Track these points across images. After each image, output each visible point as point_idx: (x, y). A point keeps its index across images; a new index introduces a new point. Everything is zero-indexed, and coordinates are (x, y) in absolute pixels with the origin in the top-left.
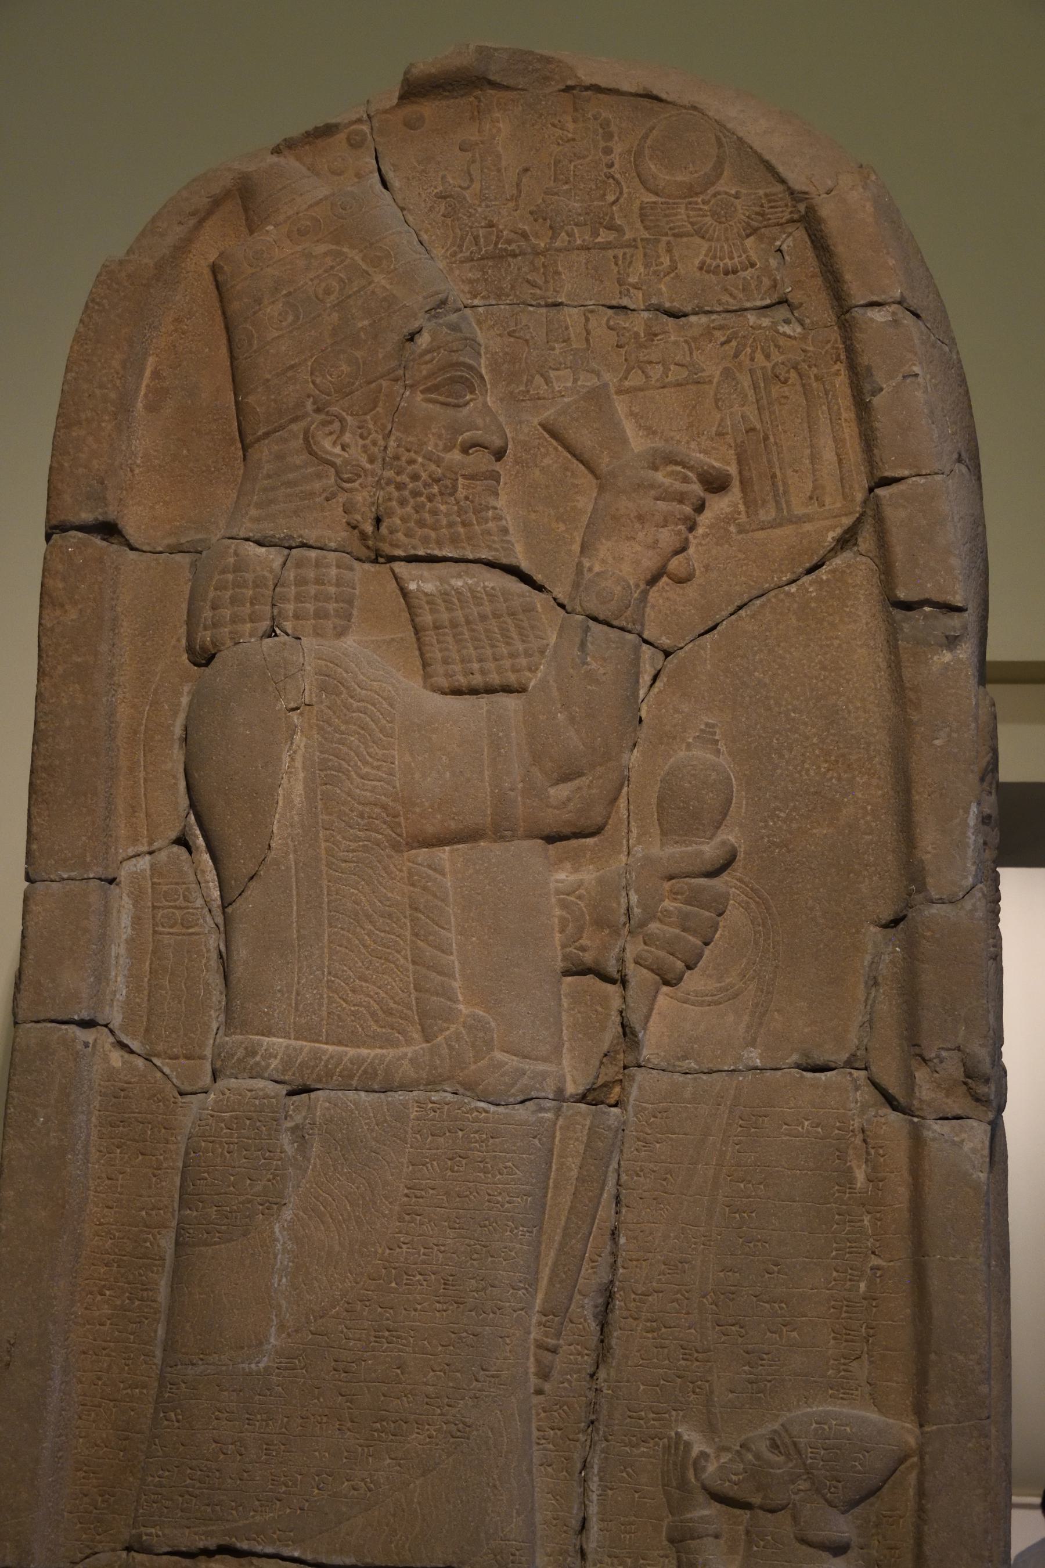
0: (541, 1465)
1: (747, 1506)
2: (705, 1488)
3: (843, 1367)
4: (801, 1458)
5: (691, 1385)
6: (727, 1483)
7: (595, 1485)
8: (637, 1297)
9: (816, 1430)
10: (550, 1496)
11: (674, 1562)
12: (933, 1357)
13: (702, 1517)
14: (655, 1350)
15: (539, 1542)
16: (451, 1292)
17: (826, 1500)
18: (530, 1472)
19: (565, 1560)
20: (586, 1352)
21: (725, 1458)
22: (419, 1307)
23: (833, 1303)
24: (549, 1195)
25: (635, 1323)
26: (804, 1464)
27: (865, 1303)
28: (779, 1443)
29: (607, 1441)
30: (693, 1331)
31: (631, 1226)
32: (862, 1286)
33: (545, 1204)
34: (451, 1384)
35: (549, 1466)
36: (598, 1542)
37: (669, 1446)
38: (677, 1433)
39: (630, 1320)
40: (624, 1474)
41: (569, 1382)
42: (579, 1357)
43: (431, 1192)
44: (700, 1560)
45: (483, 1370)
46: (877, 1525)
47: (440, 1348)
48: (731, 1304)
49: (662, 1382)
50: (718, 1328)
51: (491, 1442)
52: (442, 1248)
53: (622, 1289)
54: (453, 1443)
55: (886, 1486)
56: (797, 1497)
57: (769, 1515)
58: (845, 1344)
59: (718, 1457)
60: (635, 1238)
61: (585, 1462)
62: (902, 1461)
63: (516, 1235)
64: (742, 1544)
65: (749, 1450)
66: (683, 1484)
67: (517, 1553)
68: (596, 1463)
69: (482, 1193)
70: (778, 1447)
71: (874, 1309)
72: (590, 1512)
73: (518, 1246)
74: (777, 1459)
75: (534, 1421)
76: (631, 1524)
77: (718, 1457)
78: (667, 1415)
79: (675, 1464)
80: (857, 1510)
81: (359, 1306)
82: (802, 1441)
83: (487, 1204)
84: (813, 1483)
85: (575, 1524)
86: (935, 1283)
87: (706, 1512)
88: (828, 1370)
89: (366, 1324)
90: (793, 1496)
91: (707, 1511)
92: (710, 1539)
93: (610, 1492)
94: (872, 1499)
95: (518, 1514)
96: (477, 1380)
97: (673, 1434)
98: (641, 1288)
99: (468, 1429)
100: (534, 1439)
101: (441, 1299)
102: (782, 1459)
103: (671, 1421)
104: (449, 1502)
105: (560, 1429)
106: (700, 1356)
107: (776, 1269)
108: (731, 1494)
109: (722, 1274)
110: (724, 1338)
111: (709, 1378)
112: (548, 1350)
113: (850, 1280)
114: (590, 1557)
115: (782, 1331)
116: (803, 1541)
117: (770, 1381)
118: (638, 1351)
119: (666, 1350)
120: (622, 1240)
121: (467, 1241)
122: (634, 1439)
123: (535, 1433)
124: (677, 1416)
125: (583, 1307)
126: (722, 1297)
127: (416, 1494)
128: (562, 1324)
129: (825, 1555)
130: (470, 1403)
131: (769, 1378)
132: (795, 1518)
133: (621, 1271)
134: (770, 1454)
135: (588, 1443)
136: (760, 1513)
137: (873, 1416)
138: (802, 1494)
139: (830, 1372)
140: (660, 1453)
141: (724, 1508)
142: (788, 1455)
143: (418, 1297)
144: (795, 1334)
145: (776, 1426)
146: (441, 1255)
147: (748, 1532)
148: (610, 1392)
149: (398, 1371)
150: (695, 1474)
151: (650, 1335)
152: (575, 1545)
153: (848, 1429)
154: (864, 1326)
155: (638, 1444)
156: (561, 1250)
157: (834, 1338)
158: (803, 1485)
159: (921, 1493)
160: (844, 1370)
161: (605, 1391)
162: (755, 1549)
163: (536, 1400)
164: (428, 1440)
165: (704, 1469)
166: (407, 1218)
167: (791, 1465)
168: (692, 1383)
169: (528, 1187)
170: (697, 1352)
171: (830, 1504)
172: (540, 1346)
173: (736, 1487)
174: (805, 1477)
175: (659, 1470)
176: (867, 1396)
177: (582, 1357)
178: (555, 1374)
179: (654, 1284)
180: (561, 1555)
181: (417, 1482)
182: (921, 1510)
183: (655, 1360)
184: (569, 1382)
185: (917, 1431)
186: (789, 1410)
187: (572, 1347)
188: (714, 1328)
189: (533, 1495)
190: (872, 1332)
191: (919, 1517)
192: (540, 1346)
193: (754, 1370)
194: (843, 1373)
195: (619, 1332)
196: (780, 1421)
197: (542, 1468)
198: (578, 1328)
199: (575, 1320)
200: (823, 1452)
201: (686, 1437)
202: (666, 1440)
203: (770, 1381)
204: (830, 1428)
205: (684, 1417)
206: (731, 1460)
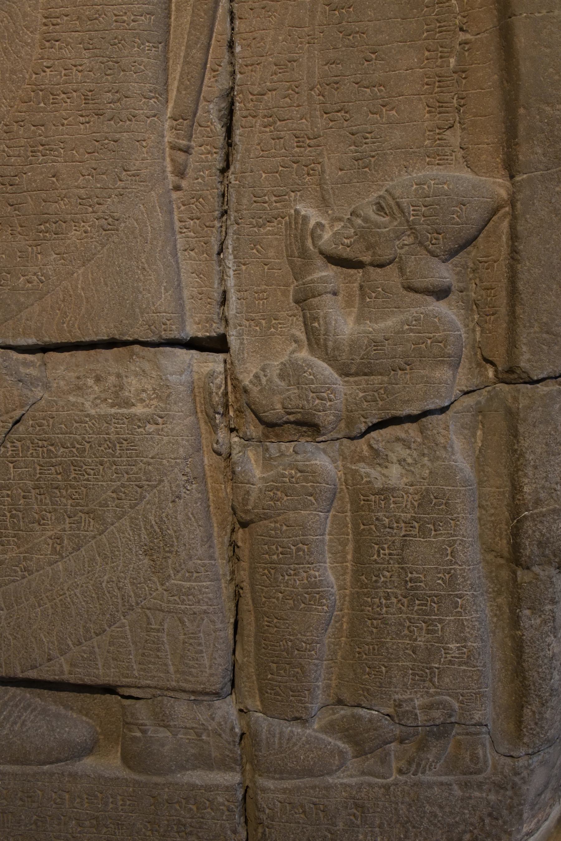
0: (185, 250)
1: (358, 265)
2: (321, 253)
3: (437, 137)
4: (404, 216)
5: (305, 168)
6: (341, 247)
7: (231, 262)
8: (254, 97)
9: (416, 190)
10: (194, 275)
11: (301, 319)
12: (522, 111)
13: (321, 278)
14: (273, 142)
15: (188, 314)
16: (91, 106)
17: (429, 251)
18: (175, 255)
19: (212, 325)
20: (215, 150)
21: (338, 226)
22: (66, 122)
23: (426, 80)
24: (173, 18)
25: (254, 120)
26: (408, 221)
27: (455, 76)
28: (384, 204)
29: (238, 224)
30: (304, 121)
31: (244, 35)
32: (452, 61)
33: (170, 25)
34: (99, 186)
35: (192, 250)
36: (237, 308)
37: (290, 223)
38: (296, 210)
39: (250, 118)
40: (255, 251)
41: (203, 177)
42: (209, 156)
43: (65, 18)
44: (322, 314)
45: (126, 171)
46: (474, 271)
47: (87, 155)
48: (336, 93)
49: (281, 168)
50: (325, 116)
51: (137, 231)
52: (80, 68)
53: (241, 92)
54: (105, 235)
55: (482, 235)
56: (403, 251)
57: (379, 270)
58: (438, 116)
59: (332, 226)
60: (249, 45)
61: (222, 244)
62: (495, 212)
63: (143, 50)
64: (357, 298)
65: (358, 216)
66: (304, 253)
67: (168, 322)
68: (230, 242)
69: (109, 14)
70: (383, 208)
71: (464, 81)
72: (229, 285)
73: (146, 60)
74: (384, 219)
75: (176, 213)
76: (264, 291)
77: (332, 226)
78: (287, 197)
79: (296, 236)
80: (456, 259)
81: (15, 127)
82: (404, 202)
83: (115, 24)
84: (416, 237)
85: (217, 296)
86: (522, 40)
87: (324, 274)
88: (425, 141)
89: (23, 141)
90: (399, 251)
91: (326, 273)
92: (329, 295)
93: (244, 268)
94: (469, 248)
95: (166, 290)
96: (121, 180)
97: (292, 211)
98: (256, 89)
99: (116, 222)
100: (177, 229)
101: (84, 113)
102: (387, 219)
103: (290, 201)
104: (106, 285)
105: (198, 219)
106: (312, 142)
107: (373, 56)
108: (345, 255)
109: (326, 67)
110: (331, 124)
111: (321, 160)
112: (180, 150)
113: (441, 57)
114: (231, 322)
115: (382, 111)
116: (410, 288)
117: (373, 157)
118: (259, 144)
119: (282, 140)
120: (238, 49)
121: (101, 59)
122: (261, 220)
123: (177, 224)
124: (295, 196)
125: (209, 112)
126: (328, 87)
127: (80, 282)
128: (192, 126)
129: (429, 299)
130: (116, 200)
131: (373, 153)
132: (401, 270)
133: (239, 76)
134: (377, 217)
135: (224, 229)
136: (371, 269)
137: (467, 175)
138: (407, 248)
139: (427, 142)
140: (283, 230)
141: (339, 269)
142: (393, 216)
143: (64, 113)
144: (394, 112)
145: (381, 193)
146: (80, 74)
147: (361, 287)
148: (237, 182)
149: (54, 179)
150: (313, 242)
151: (268, 129)
152: (219, 314)
153: (446, 187)
154: (455, 99)
155: (264, 224)
156: (186, 63)
157: (429, 112)
158: (408, 240)
159: (514, 236)
160: (439, 139)
161: (233, 182)
162: (368, 300)
163: (175, 195)
164: (84, 235)
165: (320, 237)
166: (47, 44)
167: (395, 223)
168: (306, 166)
169: (150, 7)
170: (309, 139)
171: (433, 254)
172: (174, 147)
173: (348, 249)
174: (409, 233)
175: (283, 244)
176: (461, 160)
177: (212, 155)
178: (190, 172)
179: (268, 84)
180: (207, 322)
181: (80, 272)
182: (514, 252)
183: (274, 151)
184: (203, 177)
185: (508, 184)
186: (392, 180)
187: (203, 148)
188: (322, 116)
189: (179, 275)
190: (462, 102)
191: (512, 258)
192: (174, 147)
193: (360, 149)
194: (438, 142)
195: (241, 129)
196: (384, 189)
197: (186, 253)
198: (206, 131)
199: (203, 124)
200: (424, 209)
201: (303, 213)
202: (287, 218)
203: (373, 157)
204: (428, 187)
205: (301, 196)
206: (343, 227)
